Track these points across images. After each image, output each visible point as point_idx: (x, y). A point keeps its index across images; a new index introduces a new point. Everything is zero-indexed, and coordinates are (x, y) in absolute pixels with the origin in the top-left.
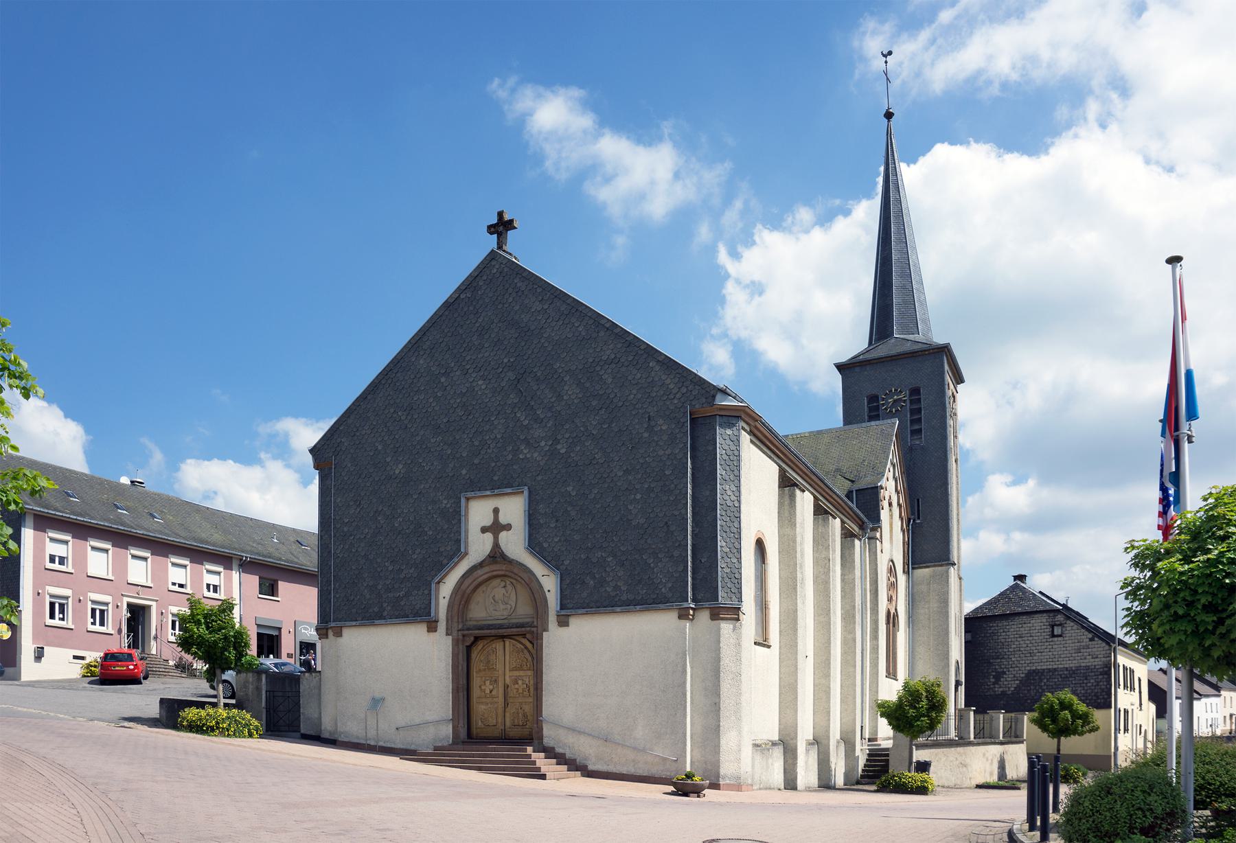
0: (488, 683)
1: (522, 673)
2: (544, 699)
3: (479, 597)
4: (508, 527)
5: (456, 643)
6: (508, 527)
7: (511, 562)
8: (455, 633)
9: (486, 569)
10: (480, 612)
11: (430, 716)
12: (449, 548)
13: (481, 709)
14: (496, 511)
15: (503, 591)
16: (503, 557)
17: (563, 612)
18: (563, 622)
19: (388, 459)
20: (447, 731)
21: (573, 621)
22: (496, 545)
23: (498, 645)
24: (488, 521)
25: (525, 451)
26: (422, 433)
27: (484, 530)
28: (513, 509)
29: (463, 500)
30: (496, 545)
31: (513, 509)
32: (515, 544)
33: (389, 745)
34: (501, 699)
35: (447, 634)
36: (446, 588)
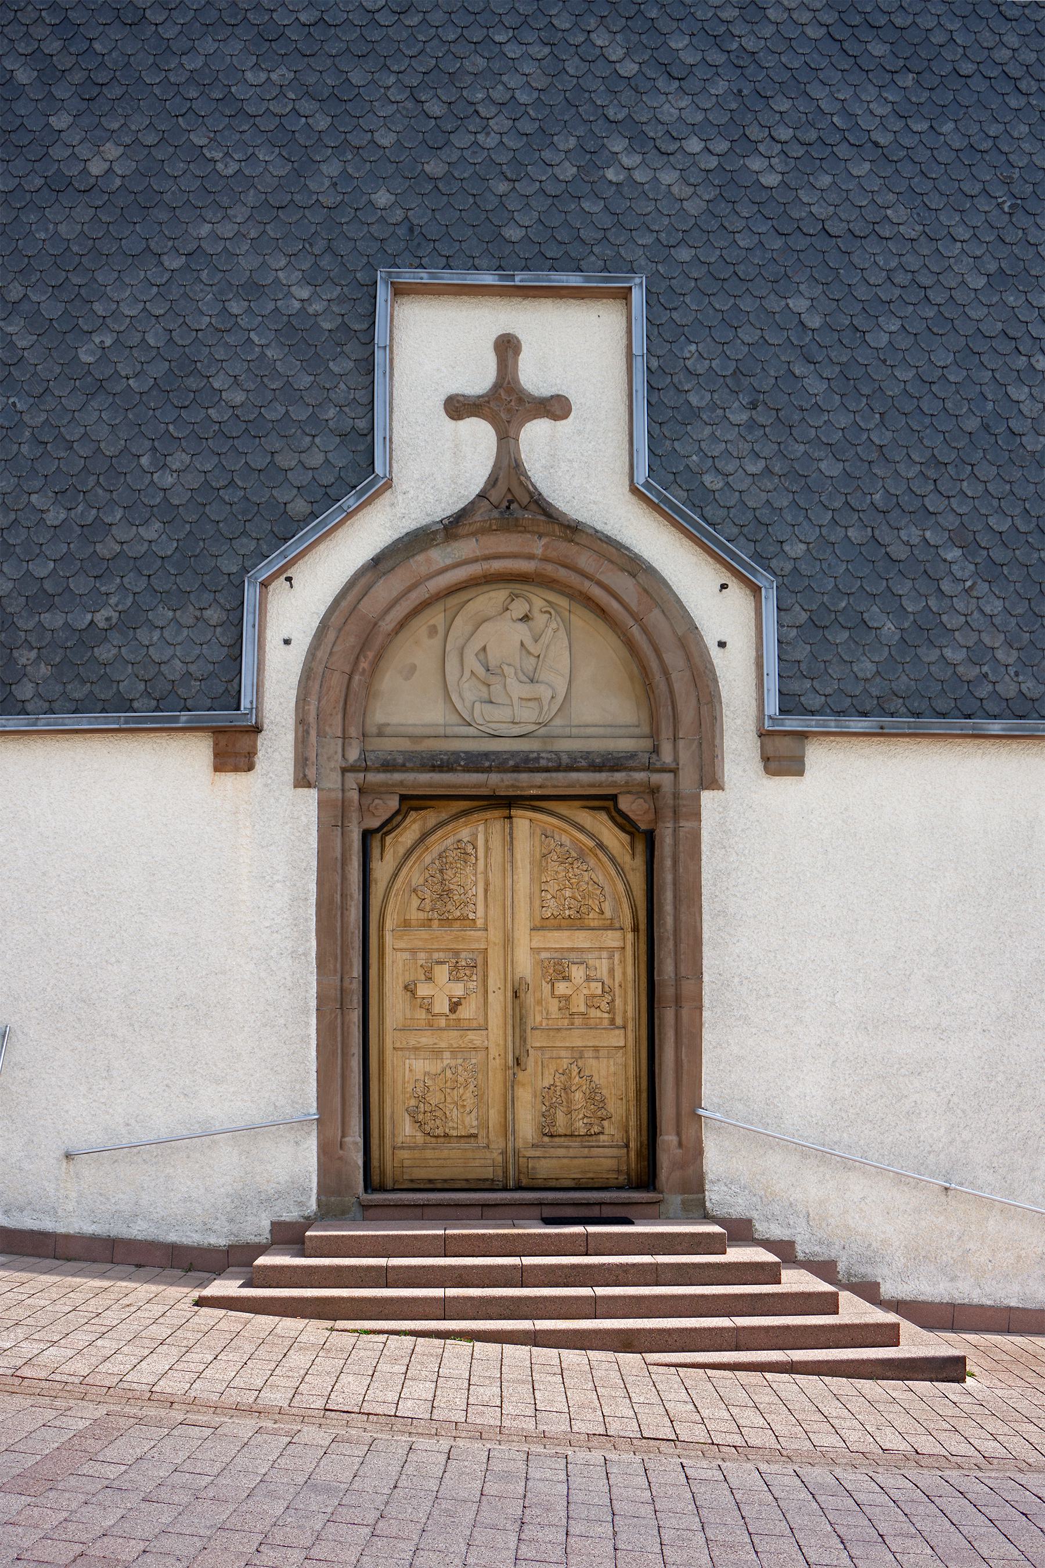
0: (442, 973)
1: (581, 939)
2: (709, 1037)
3: (417, 650)
4: (555, 407)
5: (333, 817)
6: (555, 407)
7: (573, 530)
8: (333, 781)
9: (465, 548)
10: (413, 705)
11: (224, 1104)
12: (316, 459)
13: (409, 1069)
14: (507, 348)
15: (522, 631)
16: (540, 507)
17: (793, 724)
18: (781, 757)
19: (60, 121)
20: (291, 1169)
21: (819, 757)
22: (508, 469)
23: (481, 833)
24: (478, 377)
25: (624, 163)
26: (209, 46)
27: (458, 407)
28: (581, 349)
29: (383, 293)
30: (508, 469)
31: (581, 349)
32: (588, 467)
33: (27, 1222)
34: (496, 1036)
35: (302, 781)
36: (294, 610)
